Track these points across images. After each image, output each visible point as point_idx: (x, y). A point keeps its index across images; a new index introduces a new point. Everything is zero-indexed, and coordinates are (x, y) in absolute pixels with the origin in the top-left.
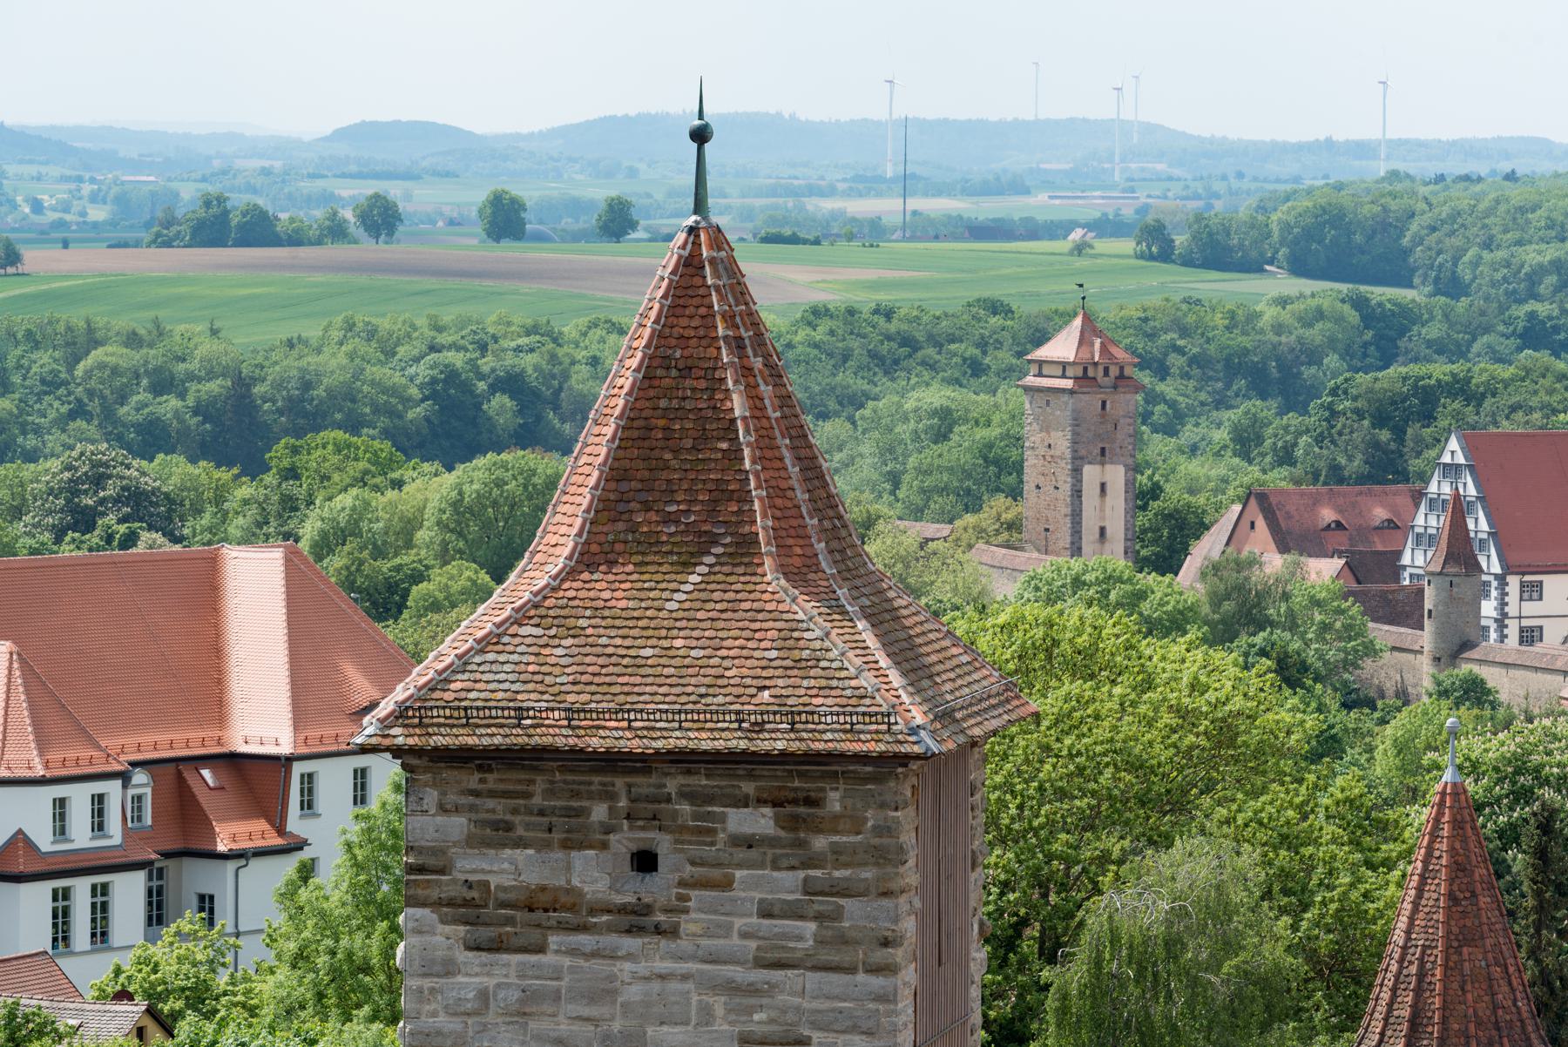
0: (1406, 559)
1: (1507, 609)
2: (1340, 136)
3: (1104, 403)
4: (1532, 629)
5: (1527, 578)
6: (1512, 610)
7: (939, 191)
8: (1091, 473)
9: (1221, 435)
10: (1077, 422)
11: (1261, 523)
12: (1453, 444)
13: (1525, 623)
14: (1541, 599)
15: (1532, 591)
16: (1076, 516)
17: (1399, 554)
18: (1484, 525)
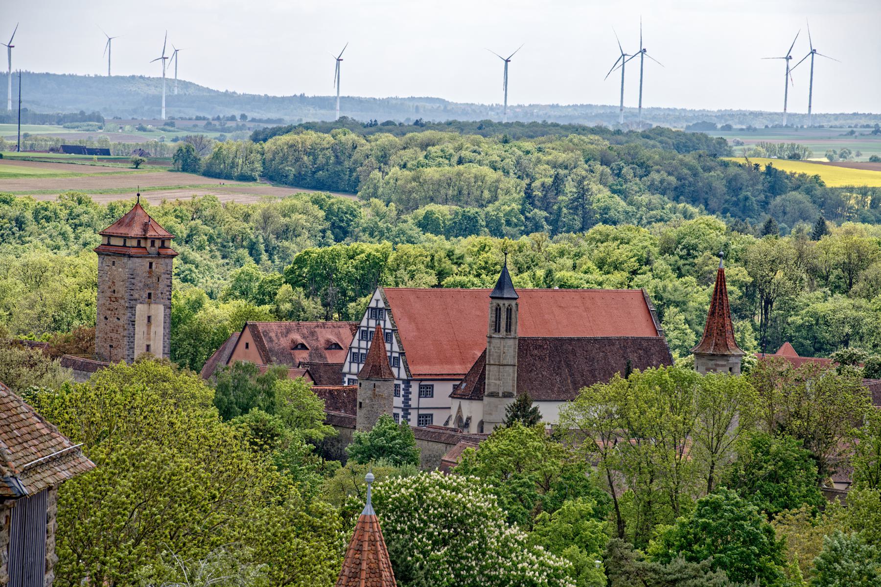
0: (346, 369)
1: (410, 402)
2: (309, 94)
3: (151, 264)
4: (426, 416)
5: (423, 383)
6: (413, 403)
7: (43, 119)
8: (141, 309)
9: (226, 285)
10: (133, 276)
11: (253, 346)
12: (378, 295)
13: (422, 412)
14: (432, 397)
15: (426, 391)
16: (132, 337)
17: (342, 365)
18: (396, 348)
